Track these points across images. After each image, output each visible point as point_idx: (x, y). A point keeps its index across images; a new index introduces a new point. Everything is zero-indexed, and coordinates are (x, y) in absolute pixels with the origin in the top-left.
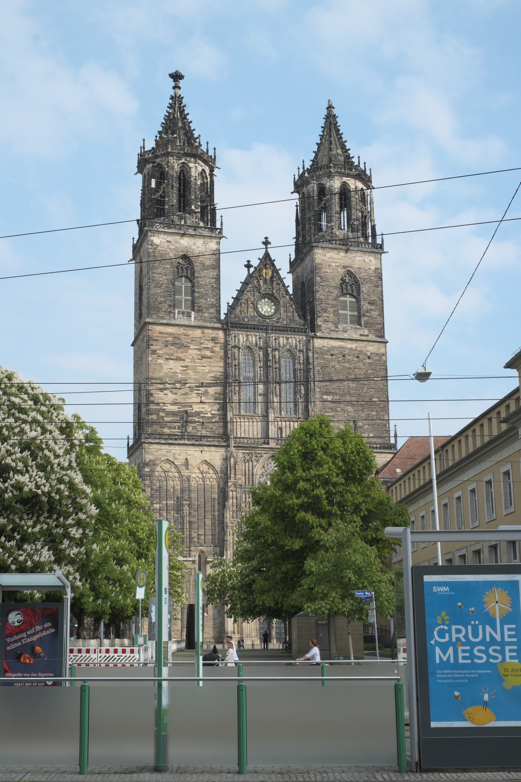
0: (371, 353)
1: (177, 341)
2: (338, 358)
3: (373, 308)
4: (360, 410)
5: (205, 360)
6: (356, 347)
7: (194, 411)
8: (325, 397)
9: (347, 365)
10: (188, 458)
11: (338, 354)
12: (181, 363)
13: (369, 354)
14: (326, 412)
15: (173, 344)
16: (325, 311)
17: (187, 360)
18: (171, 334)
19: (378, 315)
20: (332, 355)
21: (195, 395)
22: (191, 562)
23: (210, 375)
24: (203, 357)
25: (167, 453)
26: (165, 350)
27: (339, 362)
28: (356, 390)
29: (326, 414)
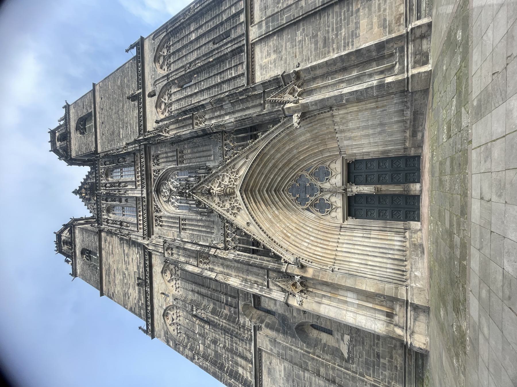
5: (114, 252)
7: (137, 271)
9: (106, 119)
10: (160, 292)
12: (116, 273)
14: (128, 134)
15: (109, 276)
16: (89, 144)
17: (114, 268)
18: (105, 276)
22: (258, 332)
23: (119, 250)
24: (112, 254)
25: (159, 314)
26: (112, 284)
27: (105, 127)
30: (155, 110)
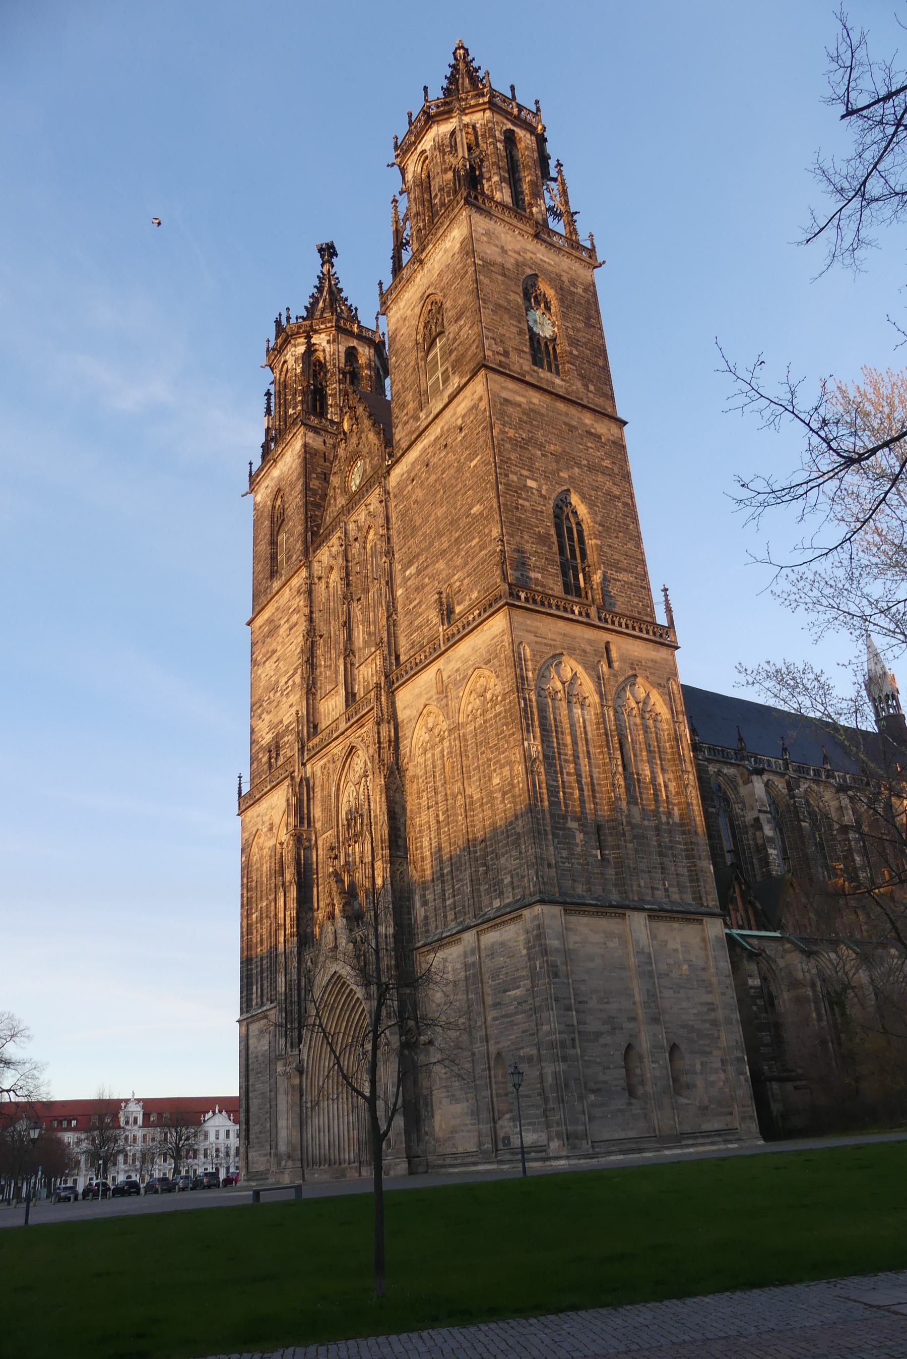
0: (464, 416)
1: (272, 625)
2: (420, 477)
3: (462, 322)
4: (455, 555)
6: (442, 429)
8: (408, 573)
11: (420, 470)
13: (459, 422)
17: (279, 649)
19: (470, 328)
20: (413, 480)
21: (284, 699)
24: (291, 629)
28: (447, 518)
29: (411, 607)
30: (422, 707)
